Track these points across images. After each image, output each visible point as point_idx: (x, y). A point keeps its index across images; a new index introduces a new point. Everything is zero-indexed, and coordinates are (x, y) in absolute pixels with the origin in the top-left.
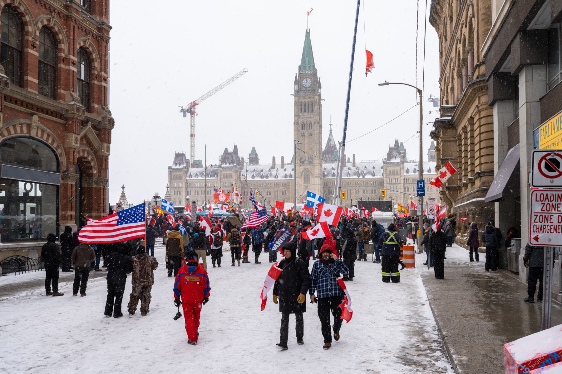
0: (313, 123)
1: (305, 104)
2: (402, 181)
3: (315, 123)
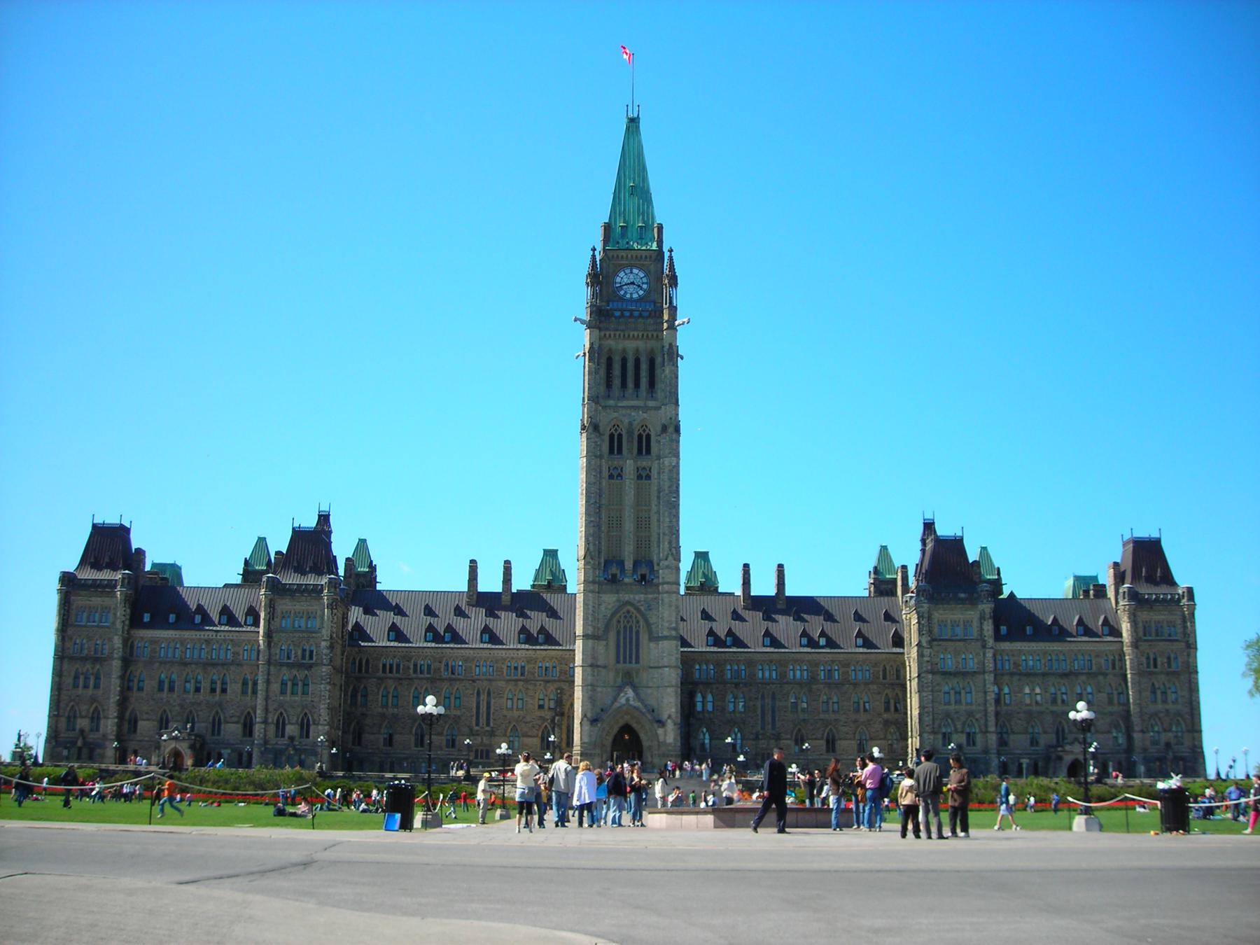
0: (654, 430)
2: (990, 666)
3: (664, 428)
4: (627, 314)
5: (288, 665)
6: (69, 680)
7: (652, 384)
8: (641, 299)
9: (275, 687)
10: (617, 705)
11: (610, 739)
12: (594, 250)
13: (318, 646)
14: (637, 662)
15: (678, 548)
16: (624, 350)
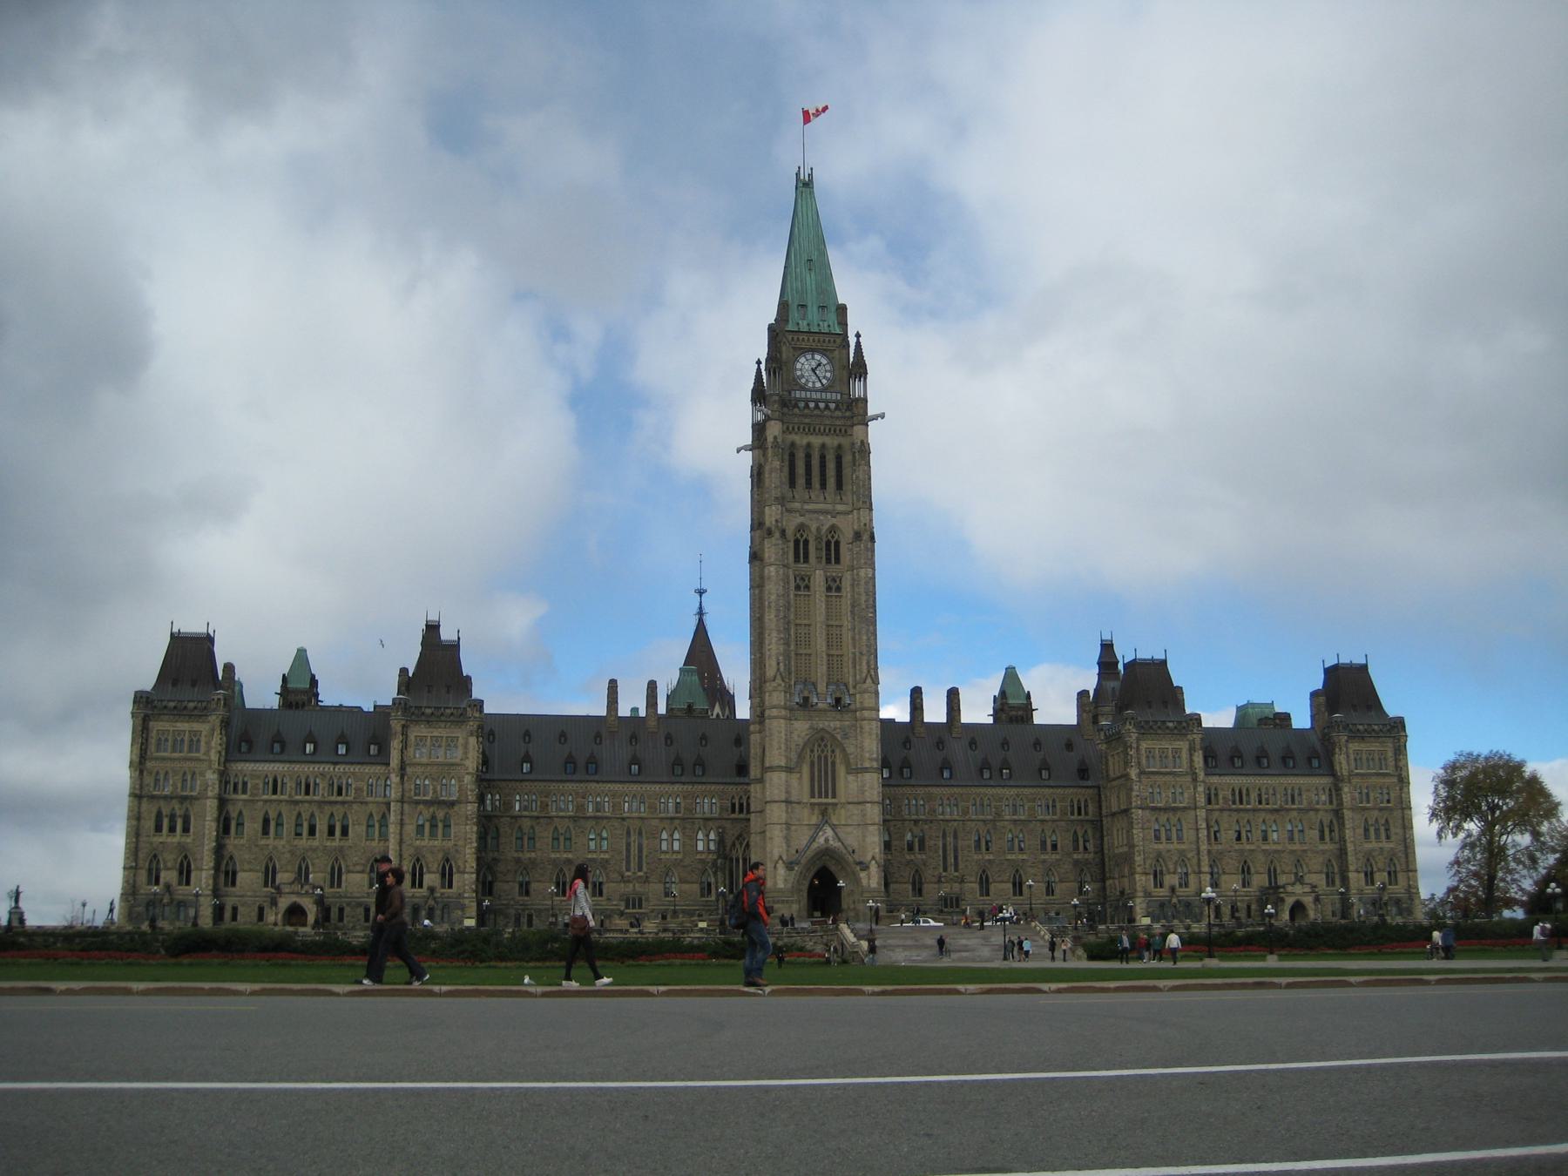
0: (846, 536)
1: (808, 457)
2: (1202, 800)
3: (858, 536)
4: (812, 405)
5: (426, 803)
6: (149, 824)
7: (839, 485)
8: (824, 389)
9: (410, 829)
10: (815, 845)
11: (806, 884)
13: (460, 780)
14: (834, 796)
15: (876, 668)
16: (809, 445)
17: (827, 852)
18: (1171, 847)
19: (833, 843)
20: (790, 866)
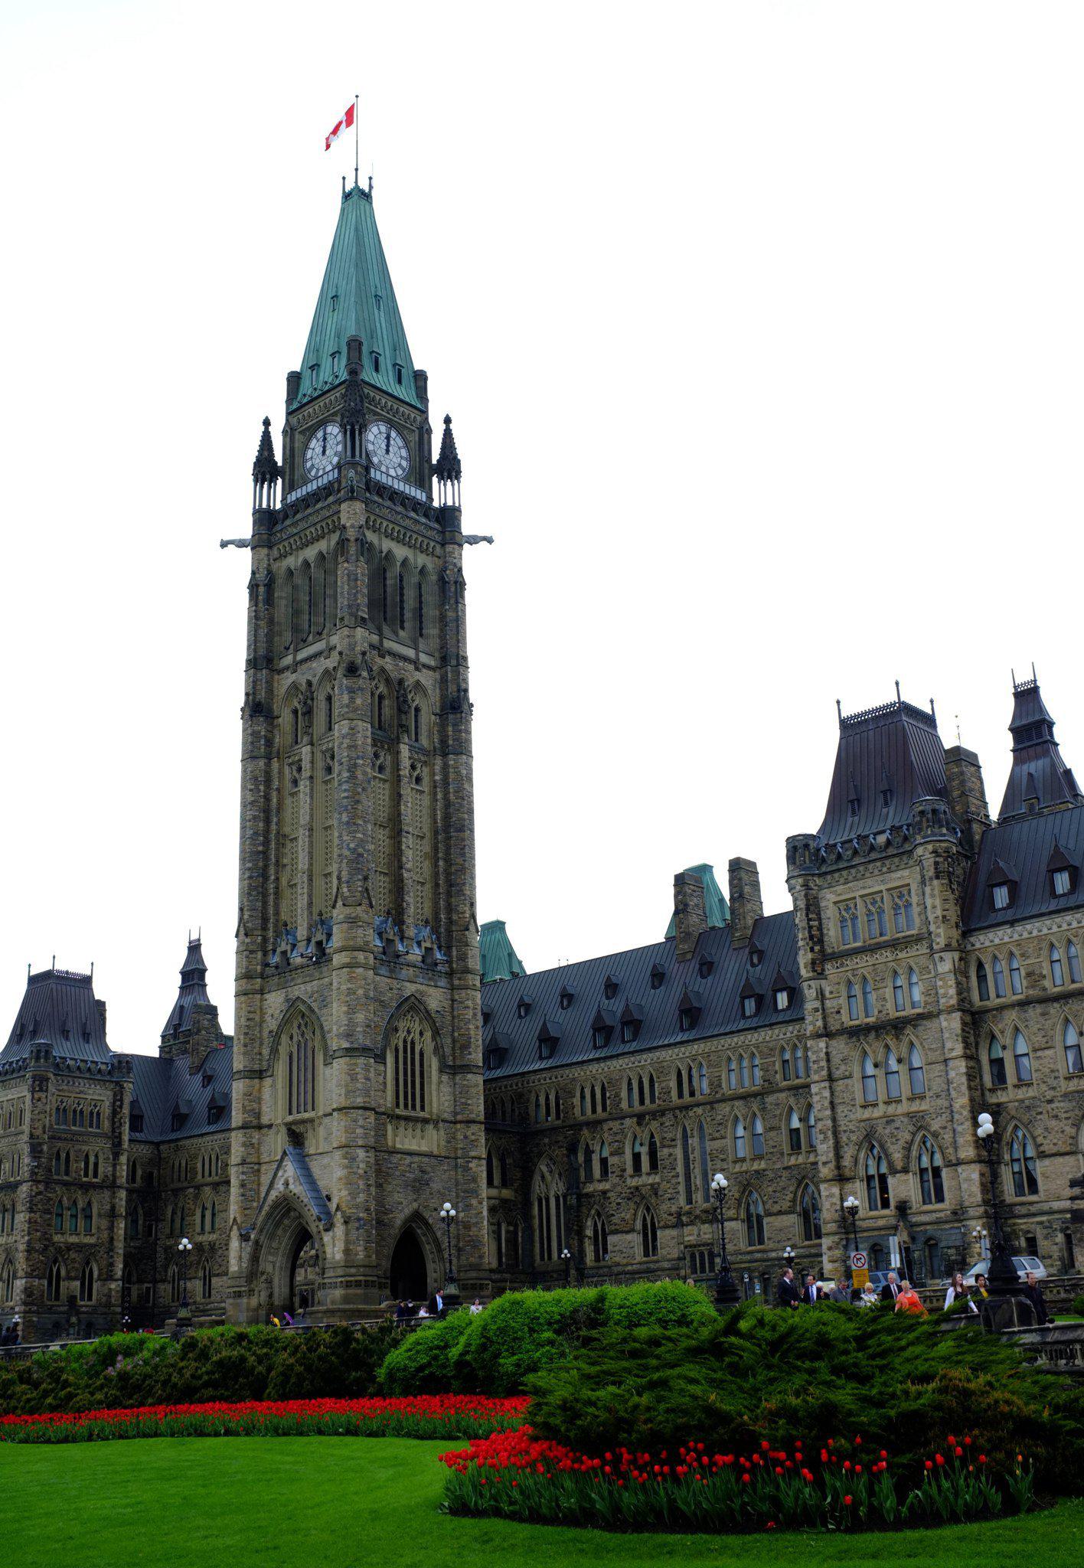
10: (273, 1194)
12: (267, 423)
17: (286, 1207)
18: (891, 1109)
19: (296, 1188)
20: (245, 1238)
